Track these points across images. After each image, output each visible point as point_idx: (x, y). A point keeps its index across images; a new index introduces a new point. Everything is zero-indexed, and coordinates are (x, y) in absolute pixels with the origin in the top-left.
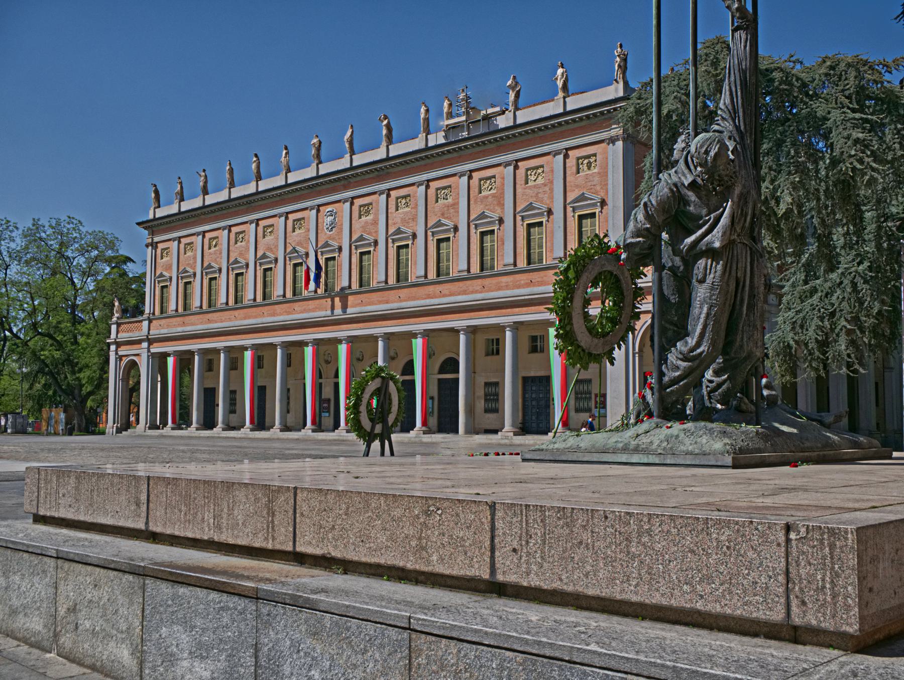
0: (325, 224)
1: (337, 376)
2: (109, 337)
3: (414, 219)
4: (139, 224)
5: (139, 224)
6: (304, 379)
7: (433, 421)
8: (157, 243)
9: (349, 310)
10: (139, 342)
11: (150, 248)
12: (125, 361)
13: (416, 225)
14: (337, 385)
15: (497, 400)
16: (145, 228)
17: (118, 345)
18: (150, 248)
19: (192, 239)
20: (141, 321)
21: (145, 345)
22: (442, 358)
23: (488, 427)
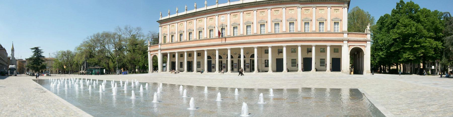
0: (221, 19)
1: (227, 58)
2: (148, 50)
4: (157, 21)
5: (157, 21)
6: (216, 59)
7: (275, 69)
8: (162, 26)
9: (226, 42)
10: (157, 50)
11: (160, 27)
12: (152, 56)
14: (227, 60)
16: (159, 23)
17: (150, 51)
18: (160, 27)
19: (174, 24)
20: (158, 45)
21: (160, 51)
22: (251, 55)
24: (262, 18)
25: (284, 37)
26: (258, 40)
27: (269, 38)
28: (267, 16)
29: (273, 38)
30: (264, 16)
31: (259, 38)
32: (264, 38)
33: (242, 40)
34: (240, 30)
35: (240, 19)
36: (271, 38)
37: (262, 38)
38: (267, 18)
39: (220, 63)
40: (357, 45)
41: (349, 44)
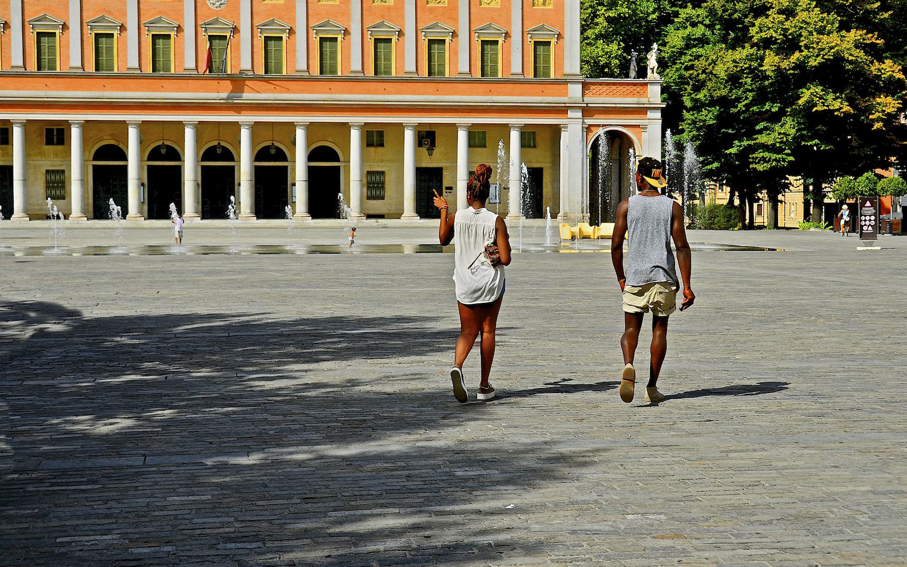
3: (347, 14)
13: (349, 20)
15: (383, 188)
23: (371, 212)
24: (383, 16)
25: (464, 93)
26: (368, 97)
27: (408, 93)
28: (403, 8)
29: (423, 94)
30: (389, 7)
31: (369, 92)
32: (388, 93)
33: (303, 92)
34: (294, 51)
35: (295, 7)
36: (414, 93)
37: (383, 94)
38: (402, 16)
39: (261, 176)
40: (616, 122)
41: (589, 121)
